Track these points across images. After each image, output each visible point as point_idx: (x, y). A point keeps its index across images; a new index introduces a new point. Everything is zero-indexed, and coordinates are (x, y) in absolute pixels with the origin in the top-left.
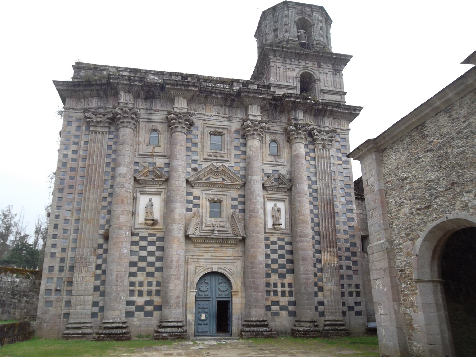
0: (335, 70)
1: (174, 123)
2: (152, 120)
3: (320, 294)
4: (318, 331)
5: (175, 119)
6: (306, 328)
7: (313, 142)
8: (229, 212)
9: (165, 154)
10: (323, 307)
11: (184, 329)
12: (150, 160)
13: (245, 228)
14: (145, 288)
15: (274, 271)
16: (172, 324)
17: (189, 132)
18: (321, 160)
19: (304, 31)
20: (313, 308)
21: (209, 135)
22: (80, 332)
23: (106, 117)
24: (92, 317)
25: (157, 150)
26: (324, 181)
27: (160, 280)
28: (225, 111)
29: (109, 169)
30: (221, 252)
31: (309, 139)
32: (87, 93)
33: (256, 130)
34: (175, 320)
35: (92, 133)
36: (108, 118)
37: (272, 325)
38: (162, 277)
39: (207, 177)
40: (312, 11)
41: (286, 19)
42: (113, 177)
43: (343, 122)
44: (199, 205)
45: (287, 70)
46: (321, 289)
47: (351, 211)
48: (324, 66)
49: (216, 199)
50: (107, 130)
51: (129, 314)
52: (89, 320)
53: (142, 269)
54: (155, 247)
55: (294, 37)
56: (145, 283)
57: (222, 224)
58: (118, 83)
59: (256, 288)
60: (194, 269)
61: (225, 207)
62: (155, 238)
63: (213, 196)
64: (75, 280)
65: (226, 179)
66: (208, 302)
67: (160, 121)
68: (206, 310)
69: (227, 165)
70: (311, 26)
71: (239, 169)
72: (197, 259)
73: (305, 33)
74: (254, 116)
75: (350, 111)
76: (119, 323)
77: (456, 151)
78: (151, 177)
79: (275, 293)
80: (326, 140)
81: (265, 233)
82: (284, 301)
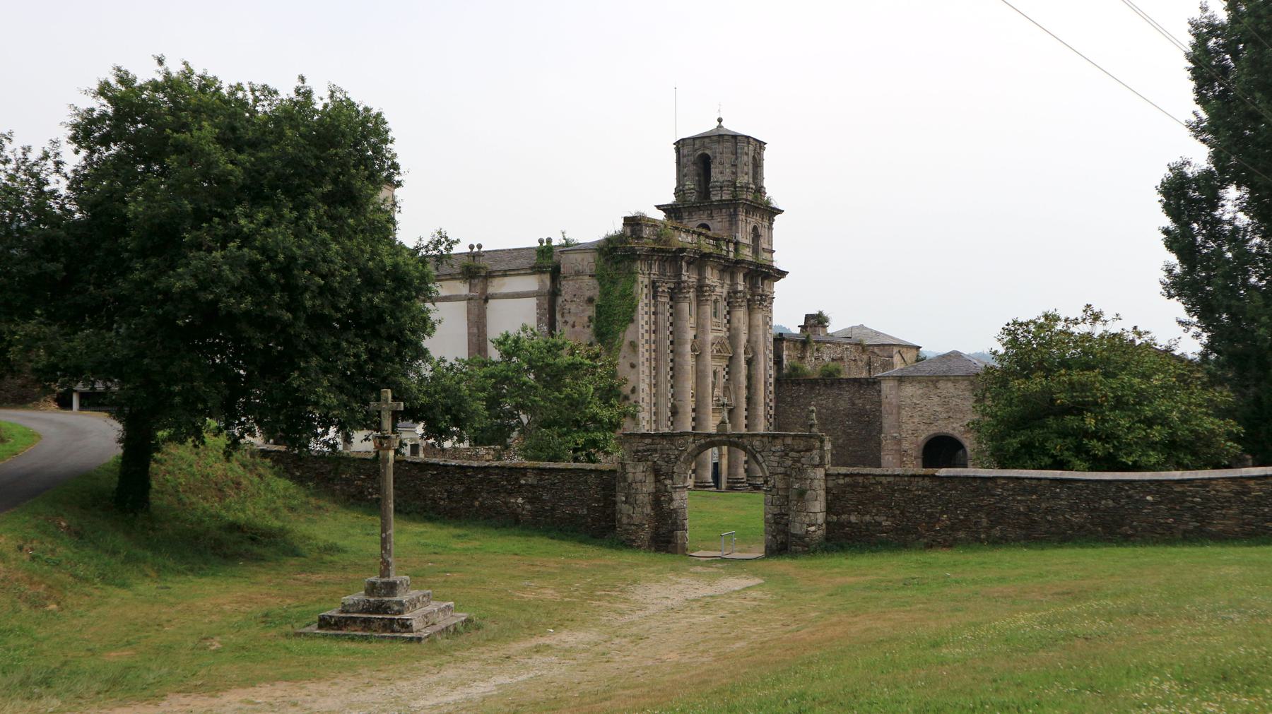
23: (668, 285)
32: (655, 258)
36: (669, 288)
41: (746, 157)
47: (770, 376)
77: (954, 403)
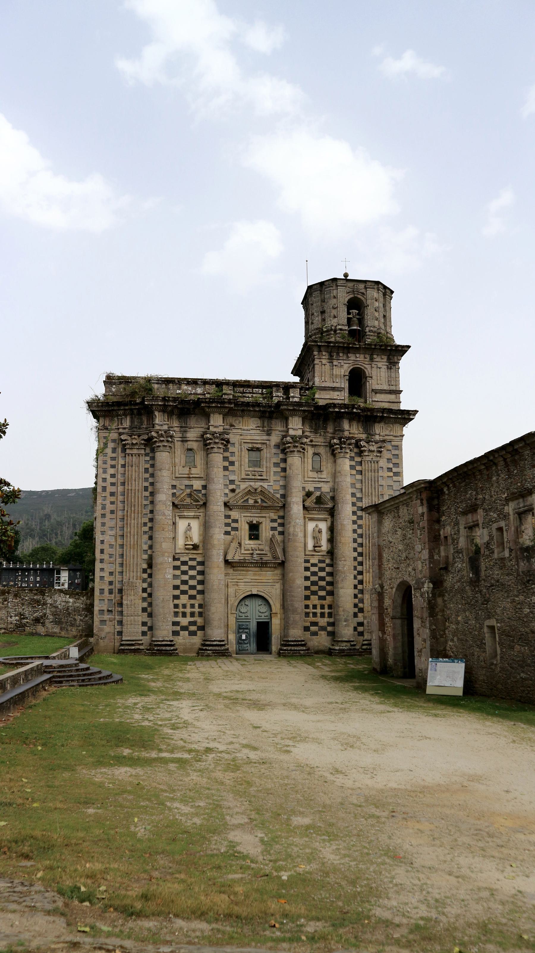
0: (390, 363)
1: (210, 443)
2: (188, 439)
3: (360, 615)
4: (355, 649)
5: (211, 439)
6: (341, 648)
7: (360, 453)
8: (268, 534)
9: (202, 476)
10: (362, 628)
11: (227, 647)
12: (187, 482)
13: (284, 551)
14: (188, 610)
15: (314, 593)
16: (215, 643)
17: (226, 450)
18: (368, 474)
19: (357, 312)
20: (351, 629)
21: (247, 452)
22: (133, 648)
23: (142, 437)
24: (142, 636)
25: (194, 471)
26: (370, 498)
27: (202, 603)
28: (263, 423)
29: (147, 494)
30: (260, 575)
31: (356, 450)
32: (121, 412)
33: (297, 447)
34: (218, 639)
35: (129, 455)
36: (143, 440)
37: (310, 644)
38: (204, 600)
39: (245, 499)
40: (366, 288)
41: (335, 300)
42: (152, 502)
43: (397, 427)
44: (237, 528)
45: (334, 367)
46: (361, 610)
48: (378, 359)
49: (255, 522)
50: (142, 452)
51: (176, 633)
52: (141, 638)
53: (184, 592)
54: (196, 571)
55: (343, 325)
56: (188, 606)
57: (261, 547)
58: (152, 405)
59: (295, 611)
60: (234, 592)
61: (264, 529)
62: (196, 562)
63: (252, 518)
64: (125, 602)
65: (265, 500)
66: (247, 623)
67: (195, 439)
68: (246, 631)
69: (265, 485)
70: (364, 307)
71: (279, 489)
72: (237, 582)
73: (358, 314)
74: (294, 429)
75: (403, 416)
76: (167, 641)
78: (188, 500)
79: (315, 615)
80: (374, 451)
81: (305, 555)
82: (323, 622)
